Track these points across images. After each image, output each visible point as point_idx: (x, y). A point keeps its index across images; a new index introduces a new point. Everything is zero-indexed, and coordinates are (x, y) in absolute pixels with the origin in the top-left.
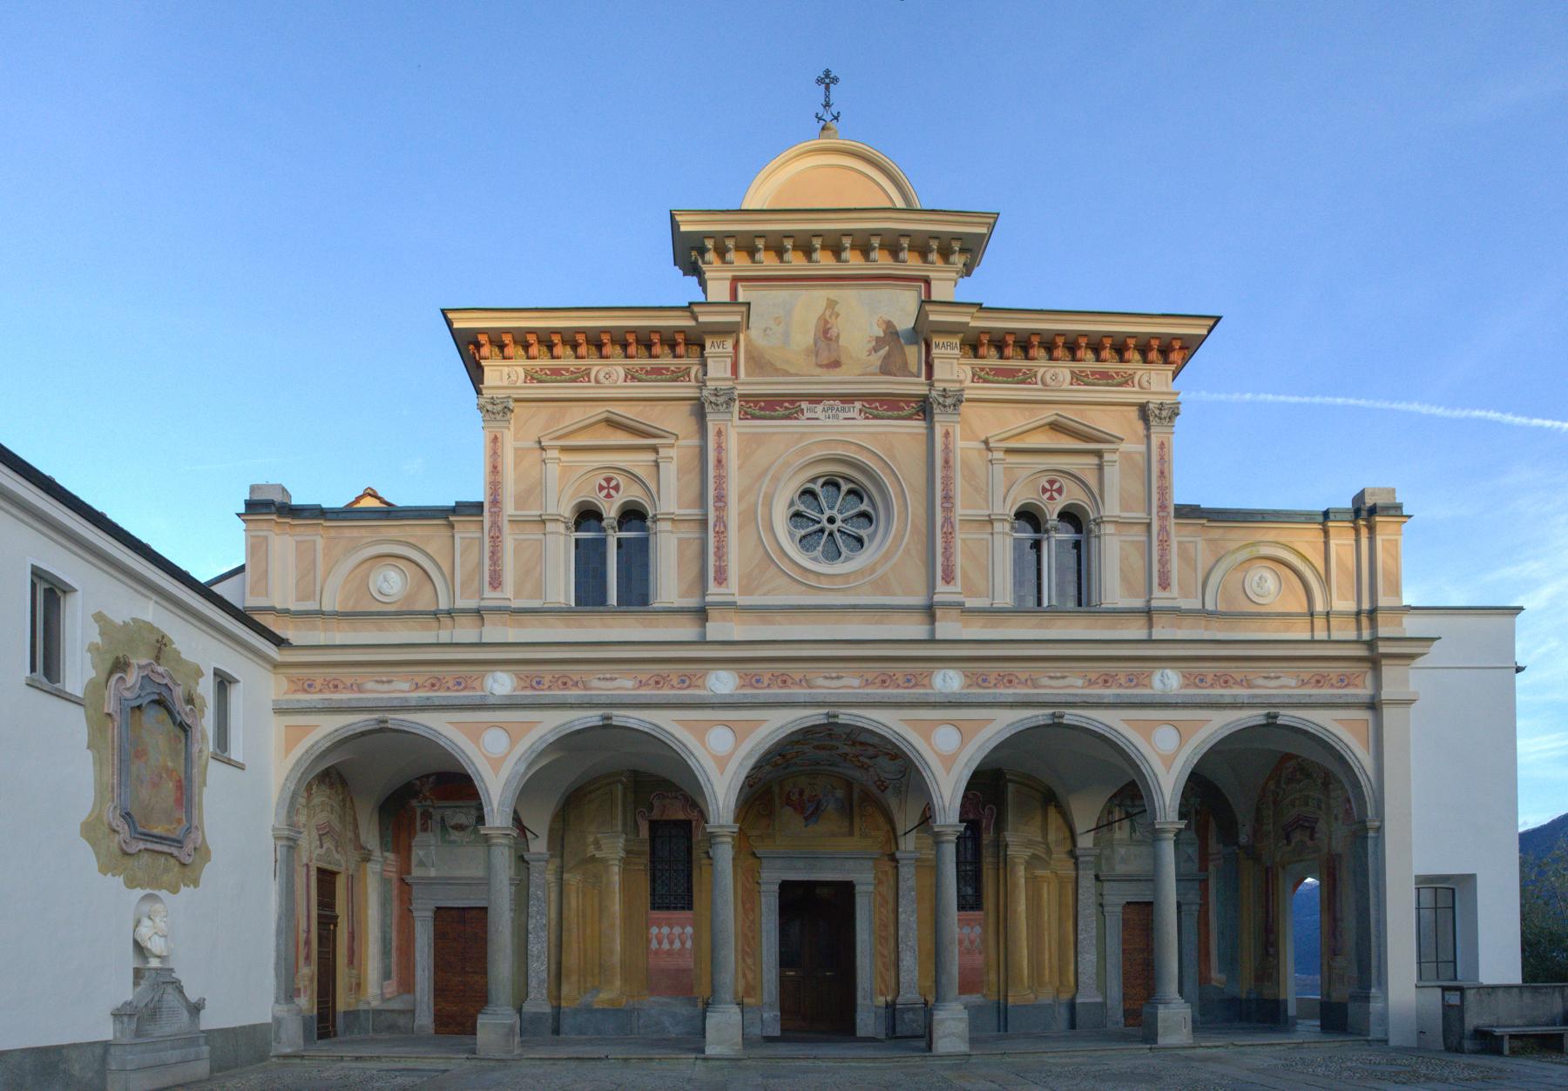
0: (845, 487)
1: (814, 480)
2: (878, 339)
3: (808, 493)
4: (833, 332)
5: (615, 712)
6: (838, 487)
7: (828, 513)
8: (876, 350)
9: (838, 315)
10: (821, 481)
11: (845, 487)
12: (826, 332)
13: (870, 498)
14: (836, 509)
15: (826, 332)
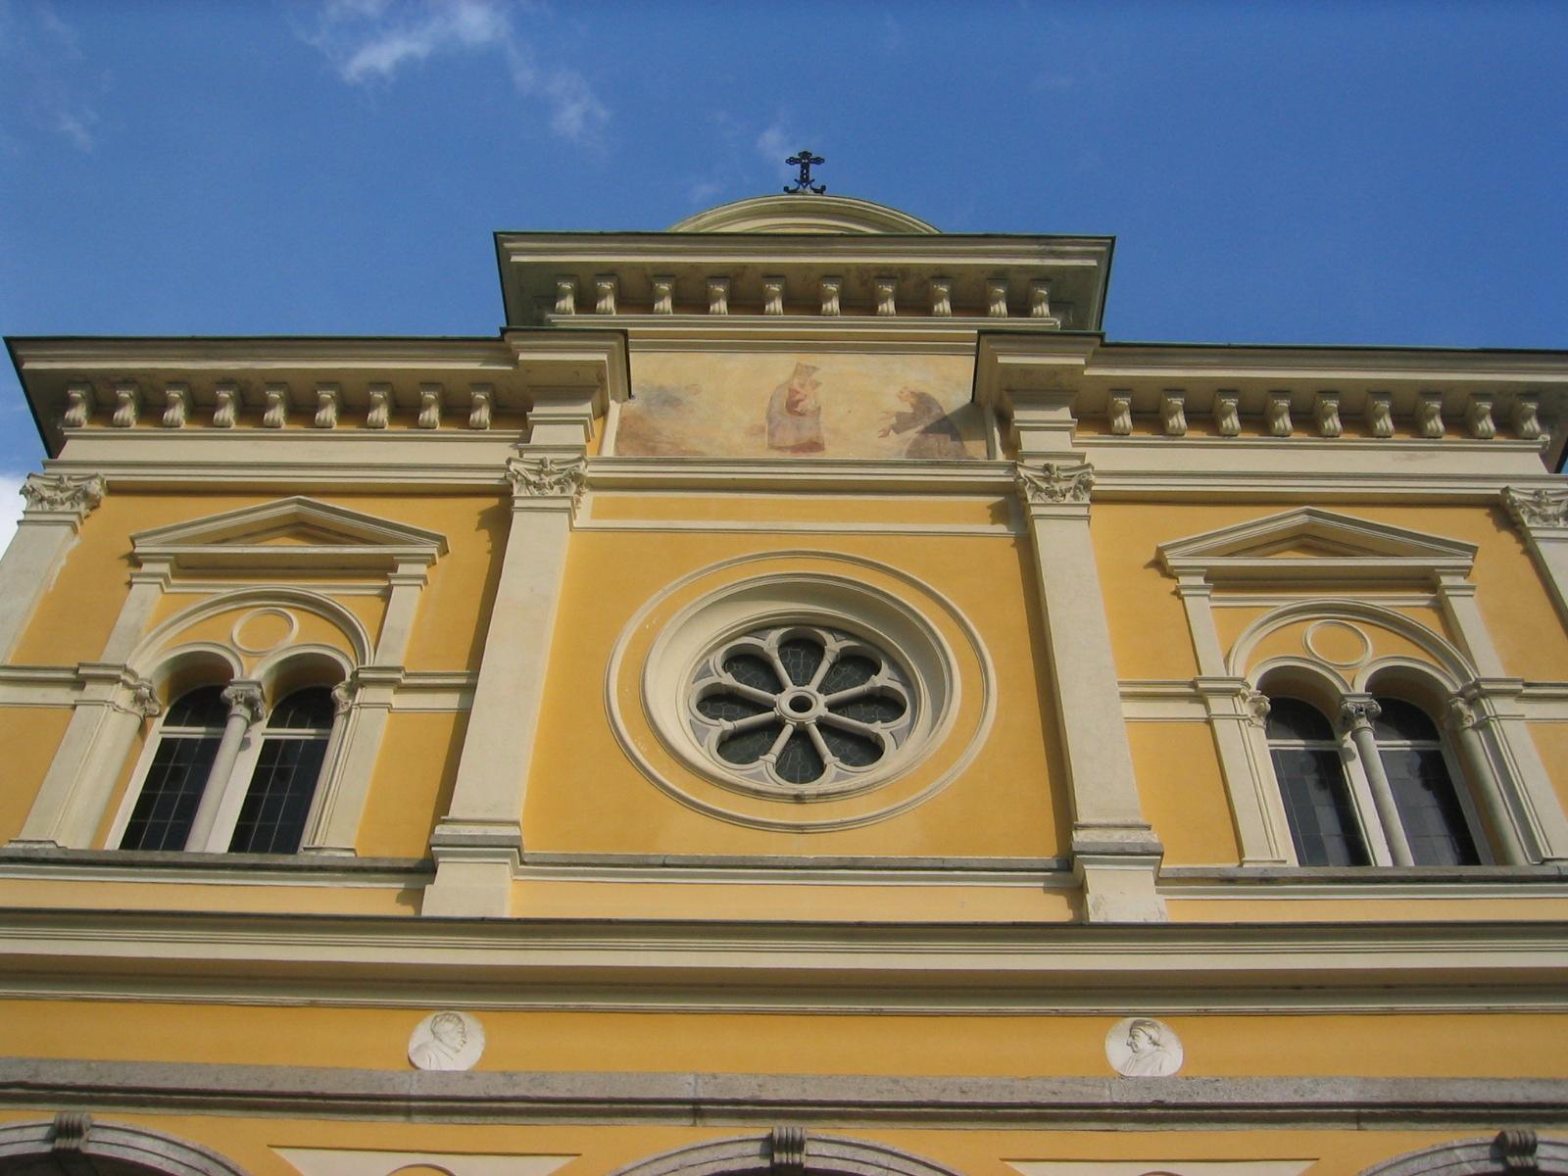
0: (833, 646)
1: (760, 629)
2: (899, 415)
3: (743, 660)
4: (808, 405)
5: (101, 1116)
6: (817, 649)
7: (783, 701)
8: (897, 429)
9: (817, 385)
10: (775, 636)
11: (833, 646)
12: (792, 406)
13: (897, 666)
14: (807, 700)
15: (792, 406)
